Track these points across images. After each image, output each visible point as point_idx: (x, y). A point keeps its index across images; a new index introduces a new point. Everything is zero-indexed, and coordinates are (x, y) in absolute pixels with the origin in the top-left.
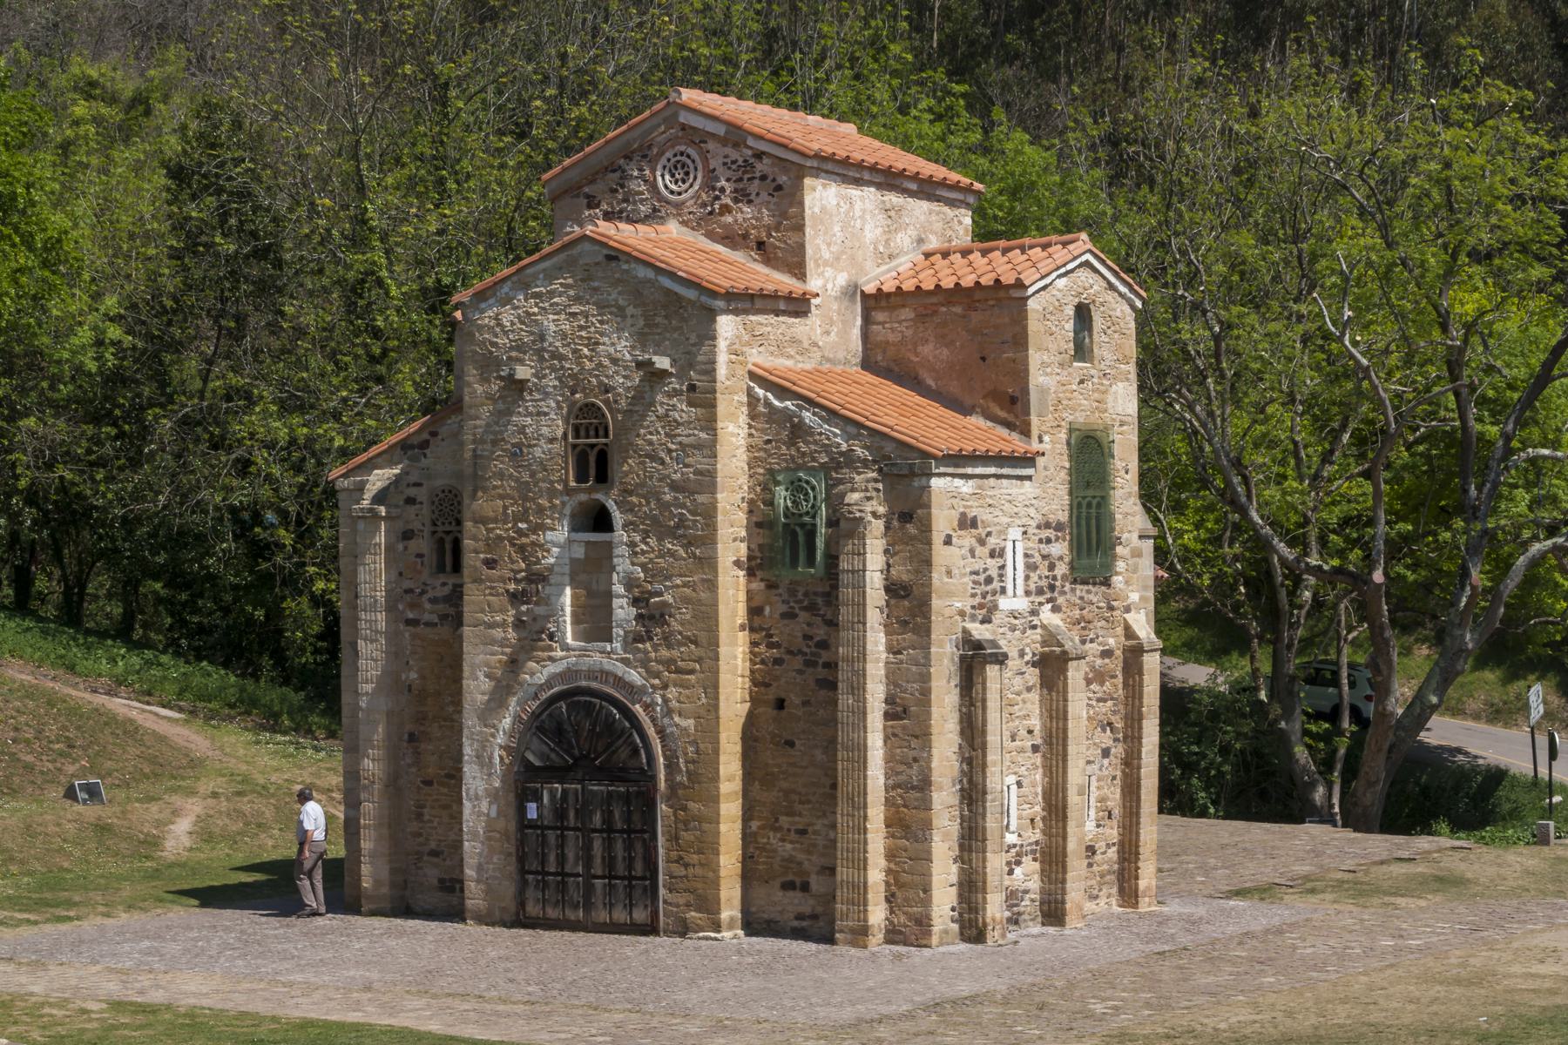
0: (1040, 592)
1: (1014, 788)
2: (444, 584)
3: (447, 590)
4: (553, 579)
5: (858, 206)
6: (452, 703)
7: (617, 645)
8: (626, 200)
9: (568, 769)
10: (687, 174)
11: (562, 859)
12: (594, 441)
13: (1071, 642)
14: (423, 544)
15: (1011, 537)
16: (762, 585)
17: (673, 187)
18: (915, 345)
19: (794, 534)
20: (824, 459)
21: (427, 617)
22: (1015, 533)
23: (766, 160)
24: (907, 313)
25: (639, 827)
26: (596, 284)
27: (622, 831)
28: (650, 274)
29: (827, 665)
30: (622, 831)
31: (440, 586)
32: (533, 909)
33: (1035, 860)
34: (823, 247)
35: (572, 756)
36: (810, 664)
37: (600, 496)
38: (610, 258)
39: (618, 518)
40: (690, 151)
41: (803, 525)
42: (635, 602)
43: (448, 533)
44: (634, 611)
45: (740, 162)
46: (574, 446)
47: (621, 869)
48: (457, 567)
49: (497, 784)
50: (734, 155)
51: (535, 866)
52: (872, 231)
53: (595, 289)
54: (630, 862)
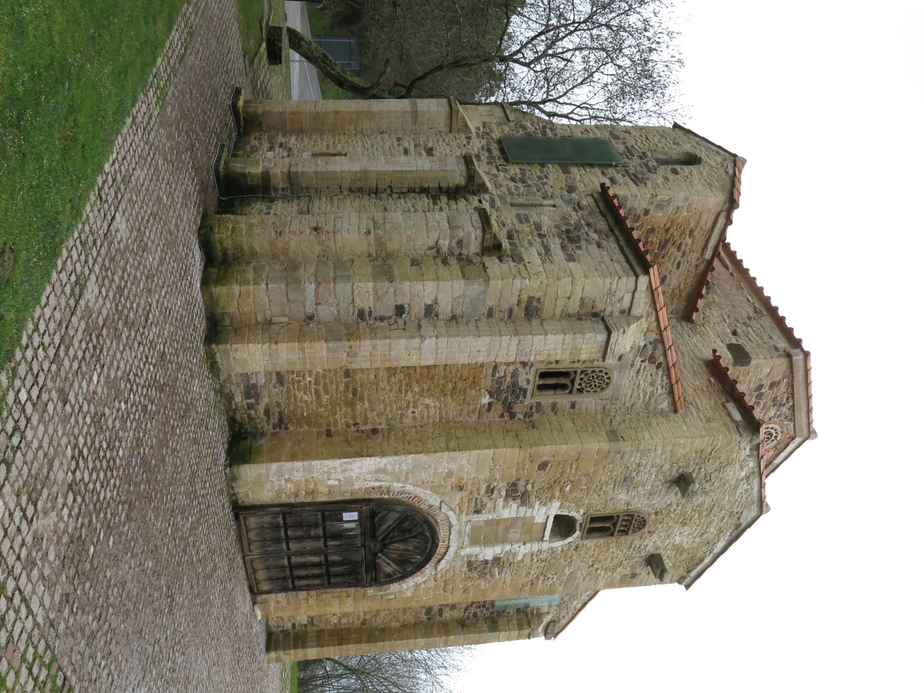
2: (528, 382)
3: (523, 384)
4: (523, 510)
6: (423, 390)
7: (468, 551)
8: (764, 407)
9: (374, 537)
11: (299, 539)
25: (332, 581)
27: (328, 572)
28: (716, 551)
30: (328, 572)
31: (527, 379)
32: (253, 521)
37: (578, 533)
38: (737, 526)
39: (559, 544)
40: (775, 441)
42: (497, 560)
43: (573, 381)
44: (490, 557)
46: (618, 516)
47: (296, 573)
48: (541, 388)
49: (356, 487)
53: (723, 518)
54: (306, 577)
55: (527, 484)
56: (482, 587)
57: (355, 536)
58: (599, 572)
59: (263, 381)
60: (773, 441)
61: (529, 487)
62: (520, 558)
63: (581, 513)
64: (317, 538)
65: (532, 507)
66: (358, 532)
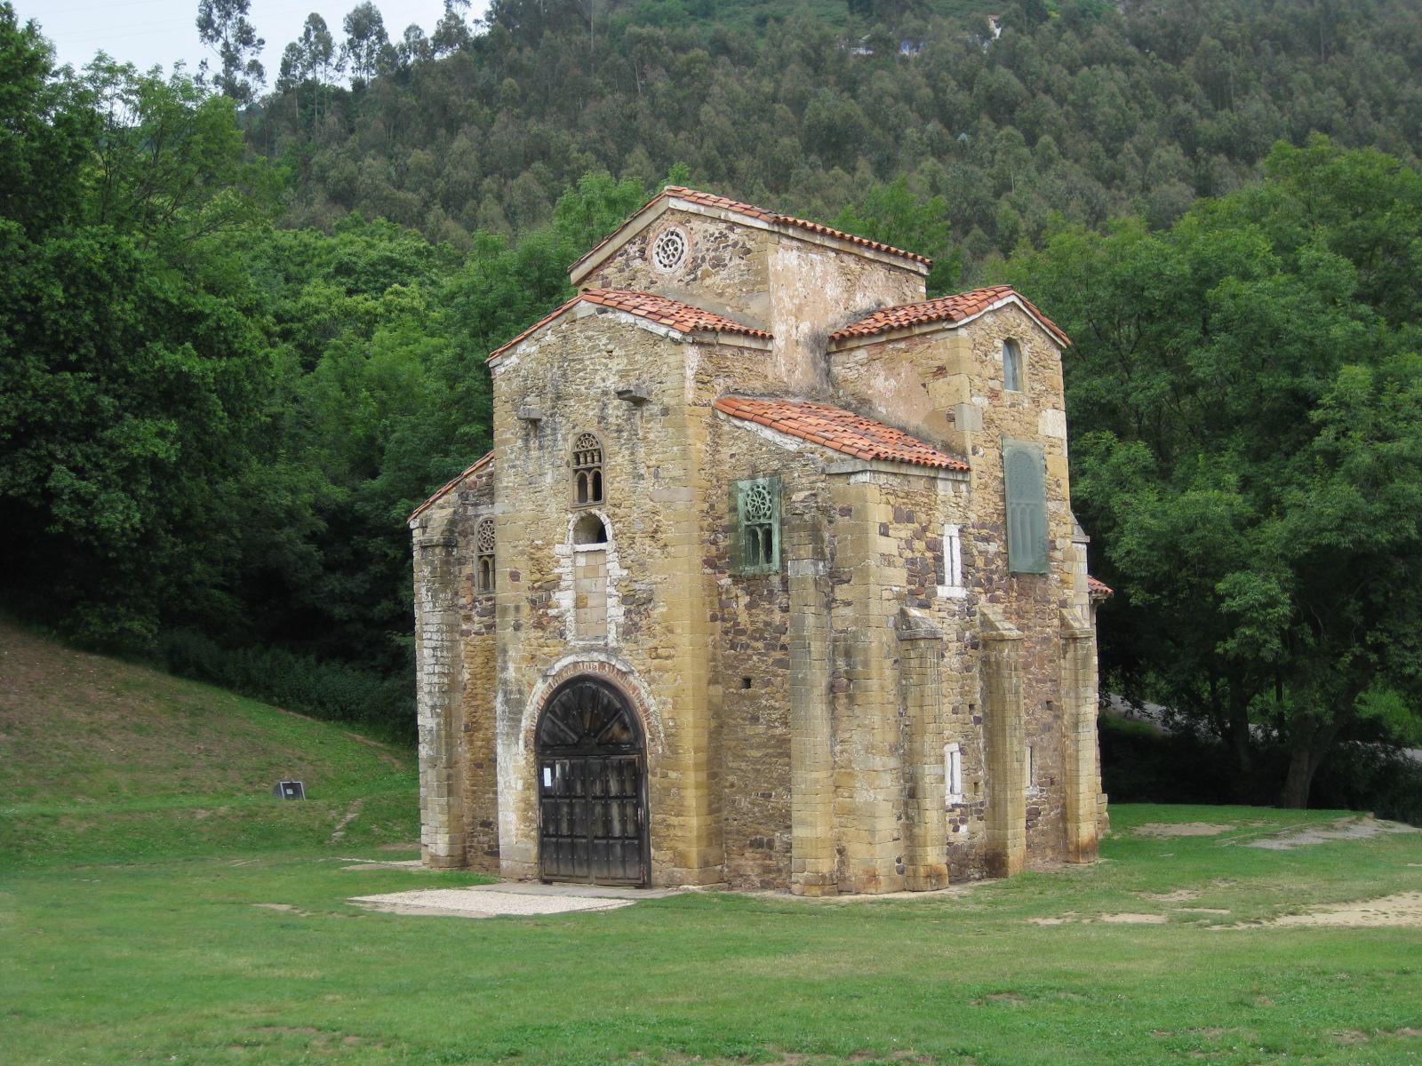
0: (979, 584)
1: (957, 756)
5: (819, 268)
10: (676, 249)
12: (590, 465)
13: (1008, 628)
14: (472, 568)
15: (947, 533)
16: (729, 581)
17: (666, 262)
18: (869, 380)
19: (755, 534)
20: (775, 464)
21: (476, 627)
22: (952, 530)
23: (738, 230)
24: (861, 355)
25: (629, 794)
26: (590, 333)
28: (631, 319)
29: (783, 647)
30: (616, 797)
33: (980, 819)
34: (786, 299)
35: (576, 733)
36: (770, 647)
37: (595, 511)
40: (678, 230)
41: (761, 526)
42: (625, 600)
44: (623, 609)
45: (717, 235)
46: (576, 471)
50: (714, 229)
51: (551, 830)
52: (833, 290)
53: (590, 338)
54: (623, 822)
55: (533, 588)
56: (664, 610)
57: (572, 766)
58: (651, 463)
59: (486, 839)
60: (677, 235)
61: (536, 585)
62: (625, 572)
63: (570, 516)
64: (571, 806)
65: (559, 577)
66: (567, 761)
